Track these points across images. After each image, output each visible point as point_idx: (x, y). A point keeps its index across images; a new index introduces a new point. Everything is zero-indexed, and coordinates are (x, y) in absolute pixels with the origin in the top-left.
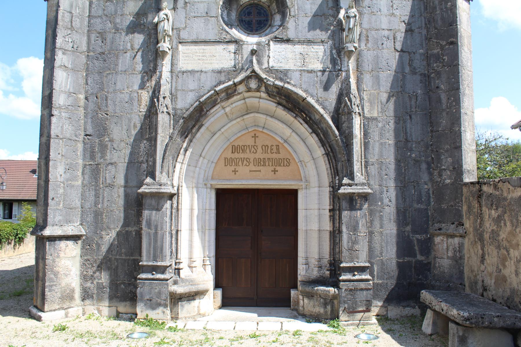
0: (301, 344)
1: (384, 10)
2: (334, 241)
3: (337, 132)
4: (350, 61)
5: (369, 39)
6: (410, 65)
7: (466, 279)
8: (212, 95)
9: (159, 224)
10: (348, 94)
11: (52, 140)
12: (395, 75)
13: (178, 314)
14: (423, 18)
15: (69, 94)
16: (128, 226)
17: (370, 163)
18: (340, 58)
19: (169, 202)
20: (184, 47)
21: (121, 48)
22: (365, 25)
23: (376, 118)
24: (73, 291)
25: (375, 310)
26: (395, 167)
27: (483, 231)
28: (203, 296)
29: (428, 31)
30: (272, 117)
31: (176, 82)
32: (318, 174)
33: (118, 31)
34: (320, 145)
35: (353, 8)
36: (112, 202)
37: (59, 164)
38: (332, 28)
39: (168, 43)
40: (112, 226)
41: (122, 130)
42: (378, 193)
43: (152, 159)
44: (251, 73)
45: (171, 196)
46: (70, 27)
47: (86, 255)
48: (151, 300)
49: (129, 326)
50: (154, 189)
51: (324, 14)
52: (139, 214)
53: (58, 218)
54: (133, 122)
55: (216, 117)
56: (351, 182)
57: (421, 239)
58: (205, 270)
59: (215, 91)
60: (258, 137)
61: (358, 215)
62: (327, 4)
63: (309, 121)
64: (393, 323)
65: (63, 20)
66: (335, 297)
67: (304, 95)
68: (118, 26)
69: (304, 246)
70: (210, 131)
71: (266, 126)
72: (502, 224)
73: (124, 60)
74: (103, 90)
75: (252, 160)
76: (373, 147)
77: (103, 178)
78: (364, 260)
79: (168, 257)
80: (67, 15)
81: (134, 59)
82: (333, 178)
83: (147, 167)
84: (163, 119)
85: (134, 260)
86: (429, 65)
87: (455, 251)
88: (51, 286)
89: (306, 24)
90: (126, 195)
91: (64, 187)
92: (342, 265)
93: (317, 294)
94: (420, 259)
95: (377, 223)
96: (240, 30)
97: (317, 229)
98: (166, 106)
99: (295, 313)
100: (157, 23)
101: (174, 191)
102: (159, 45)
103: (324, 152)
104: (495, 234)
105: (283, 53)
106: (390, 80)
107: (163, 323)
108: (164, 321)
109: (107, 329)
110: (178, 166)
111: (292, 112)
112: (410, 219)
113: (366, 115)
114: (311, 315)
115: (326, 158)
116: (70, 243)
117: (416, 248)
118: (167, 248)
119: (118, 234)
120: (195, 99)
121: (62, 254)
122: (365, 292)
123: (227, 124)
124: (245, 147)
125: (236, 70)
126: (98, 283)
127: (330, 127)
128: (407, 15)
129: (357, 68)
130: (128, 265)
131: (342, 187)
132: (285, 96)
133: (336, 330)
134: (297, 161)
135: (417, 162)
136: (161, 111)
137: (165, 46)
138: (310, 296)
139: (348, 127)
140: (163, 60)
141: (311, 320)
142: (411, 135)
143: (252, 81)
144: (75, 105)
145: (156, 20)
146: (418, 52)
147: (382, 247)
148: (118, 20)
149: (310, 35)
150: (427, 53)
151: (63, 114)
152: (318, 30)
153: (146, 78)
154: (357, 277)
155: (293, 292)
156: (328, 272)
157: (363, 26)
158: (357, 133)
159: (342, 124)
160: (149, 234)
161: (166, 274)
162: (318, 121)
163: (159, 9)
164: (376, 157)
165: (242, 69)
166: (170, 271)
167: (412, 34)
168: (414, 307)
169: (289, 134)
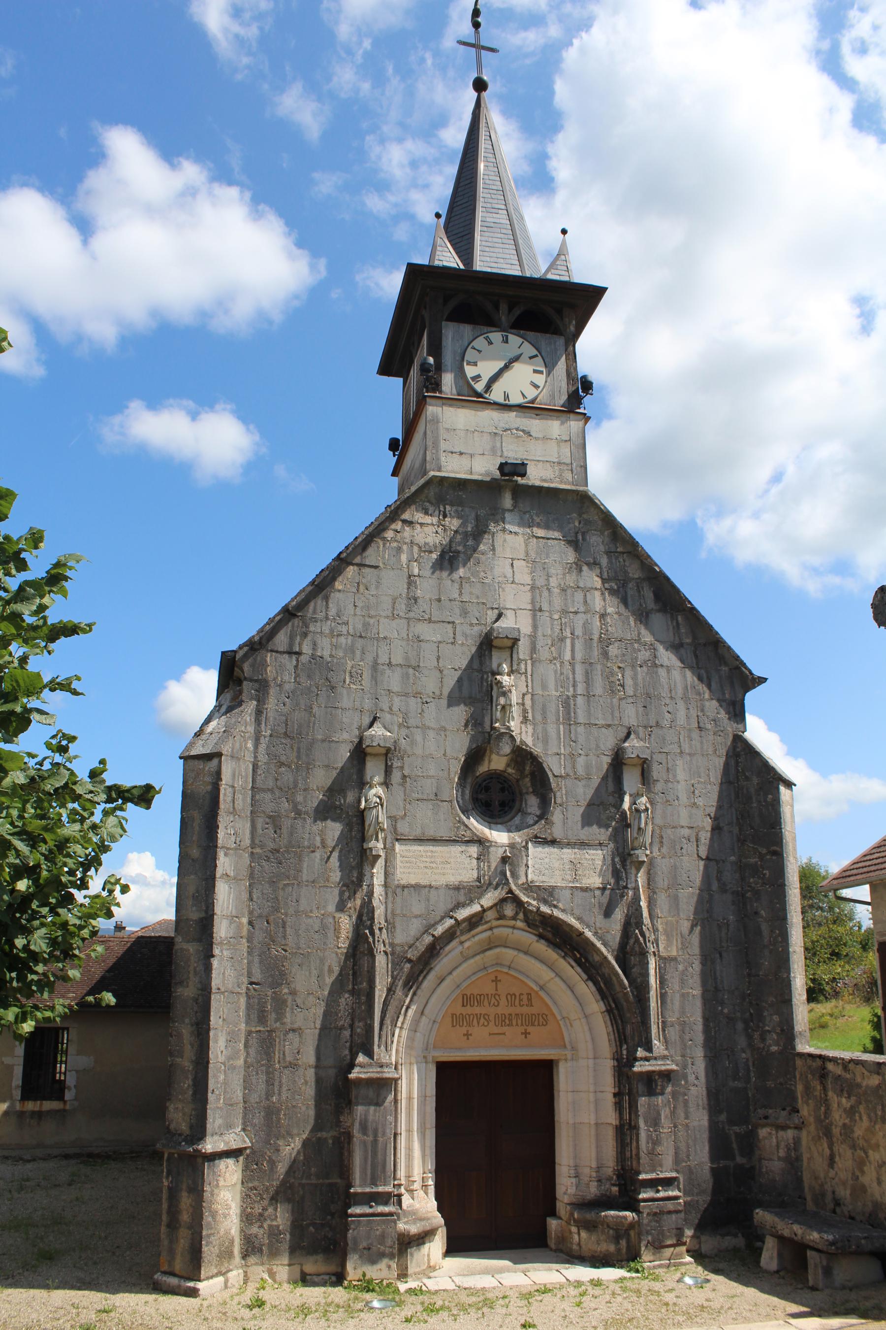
5: (664, 841)
7: (806, 1190)
9: (380, 1126)
10: (639, 924)
11: (213, 997)
12: (699, 895)
13: (407, 1268)
14: (733, 810)
15: (232, 918)
17: (669, 1024)
20: (403, 847)
21: (306, 843)
22: (659, 821)
24: (232, 1242)
27: (831, 1124)
29: (740, 830)
30: (526, 953)
31: (393, 903)
32: (593, 1039)
34: (599, 997)
36: (295, 1091)
37: (220, 1034)
38: (614, 823)
40: (295, 1131)
46: (232, 809)
47: (251, 1179)
48: (369, 1249)
51: (602, 803)
53: (219, 1121)
54: (327, 965)
56: (648, 1054)
61: (660, 1101)
65: (225, 800)
66: (632, 1225)
68: (300, 807)
71: (512, 965)
72: (857, 1118)
74: (277, 910)
75: (492, 1018)
76: (672, 1000)
77: (279, 1053)
80: (230, 790)
81: (326, 862)
83: (351, 1036)
84: (380, 962)
85: (331, 1185)
86: (743, 879)
87: (789, 1149)
88: (209, 1236)
90: (319, 1081)
91: (225, 1071)
95: (681, 1113)
96: (478, 818)
97: (593, 1122)
103: (604, 1009)
104: (847, 1130)
105: (547, 860)
111: (559, 948)
114: (593, 1257)
115: (608, 1018)
116: (230, 1161)
117: (735, 1146)
119: (305, 1144)
120: (422, 930)
121: (221, 1183)
122: (674, 1216)
123: (460, 965)
126: (270, 1226)
129: (649, 884)
134: (559, 1018)
135: (731, 1020)
137: (377, 846)
138: (590, 1226)
139: (640, 974)
140: (373, 867)
144: (238, 936)
147: (688, 1147)
148: (299, 798)
150: (740, 861)
151: (225, 953)
152: (595, 826)
153: (347, 894)
154: (661, 1194)
155: (553, 1224)
160: (364, 1143)
163: (362, 784)
164: (677, 1015)
165: (490, 884)
168: (736, 1236)
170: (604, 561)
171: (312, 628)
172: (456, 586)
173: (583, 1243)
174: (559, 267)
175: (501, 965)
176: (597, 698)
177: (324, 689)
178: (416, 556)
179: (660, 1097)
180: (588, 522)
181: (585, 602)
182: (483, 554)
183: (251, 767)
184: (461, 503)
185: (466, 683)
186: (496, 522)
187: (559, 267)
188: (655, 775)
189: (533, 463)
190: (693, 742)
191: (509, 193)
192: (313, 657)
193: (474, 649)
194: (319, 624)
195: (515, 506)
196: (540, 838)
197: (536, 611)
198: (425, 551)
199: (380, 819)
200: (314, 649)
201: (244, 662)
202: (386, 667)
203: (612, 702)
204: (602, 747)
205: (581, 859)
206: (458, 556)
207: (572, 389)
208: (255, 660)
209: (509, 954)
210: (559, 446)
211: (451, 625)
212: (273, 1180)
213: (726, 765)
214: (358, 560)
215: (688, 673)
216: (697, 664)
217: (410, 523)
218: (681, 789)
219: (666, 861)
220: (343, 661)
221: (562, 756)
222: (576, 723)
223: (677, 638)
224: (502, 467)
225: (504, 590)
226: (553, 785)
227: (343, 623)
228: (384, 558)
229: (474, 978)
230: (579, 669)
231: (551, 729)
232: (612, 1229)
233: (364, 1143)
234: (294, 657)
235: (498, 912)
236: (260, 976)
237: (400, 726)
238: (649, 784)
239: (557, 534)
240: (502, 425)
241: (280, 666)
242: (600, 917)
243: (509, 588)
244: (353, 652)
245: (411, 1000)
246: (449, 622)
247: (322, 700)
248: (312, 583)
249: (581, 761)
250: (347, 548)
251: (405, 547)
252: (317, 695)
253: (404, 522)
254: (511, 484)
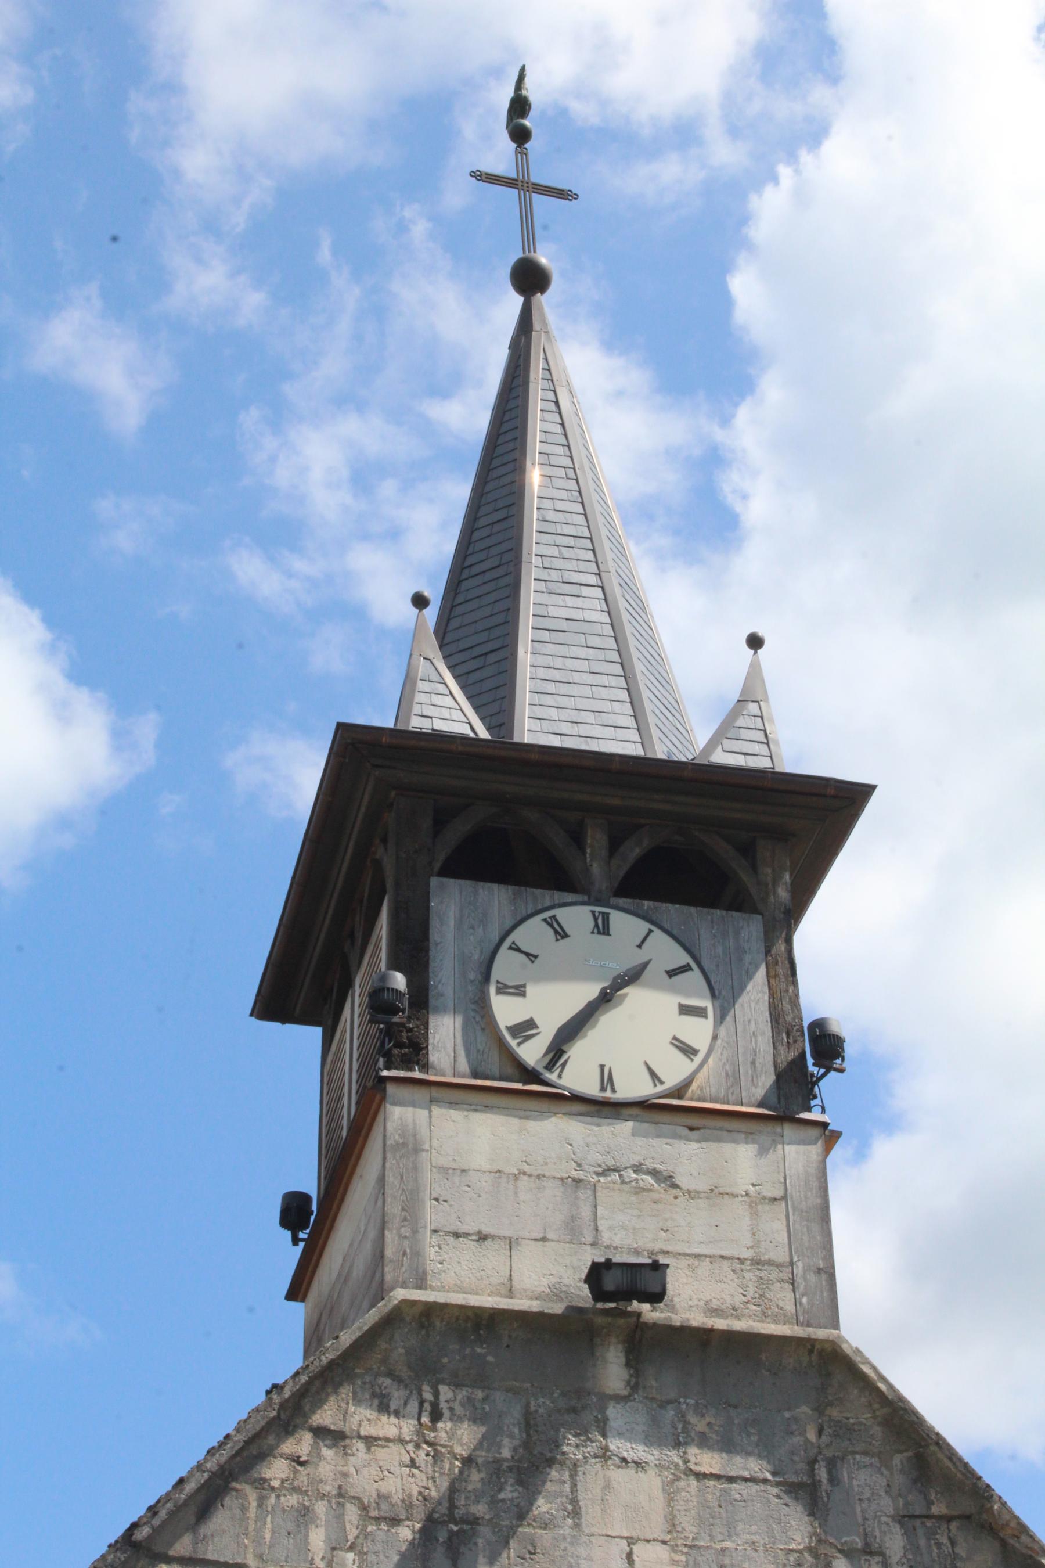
170: (895, 1543)
174: (744, 734)
178: (352, 1533)
180: (843, 1430)
182: (545, 1526)
184: (481, 1379)
186: (582, 1432)
187: (744, 734)
189: (684, 1262)
191: (607, 544)
195: (634, 1387)
198: (378, 1520)
206: (475, 1534)
207: (787, 1056)
210: (755, 1214)
217: (336, 1437)
224: (596, 1274)
228: (258, 1540)
239: (755, 1466)
240: (595, 1157)
250: (153, 1510)
251: (321, 1508)
253: (321, 1432)
254: (621, 1321)
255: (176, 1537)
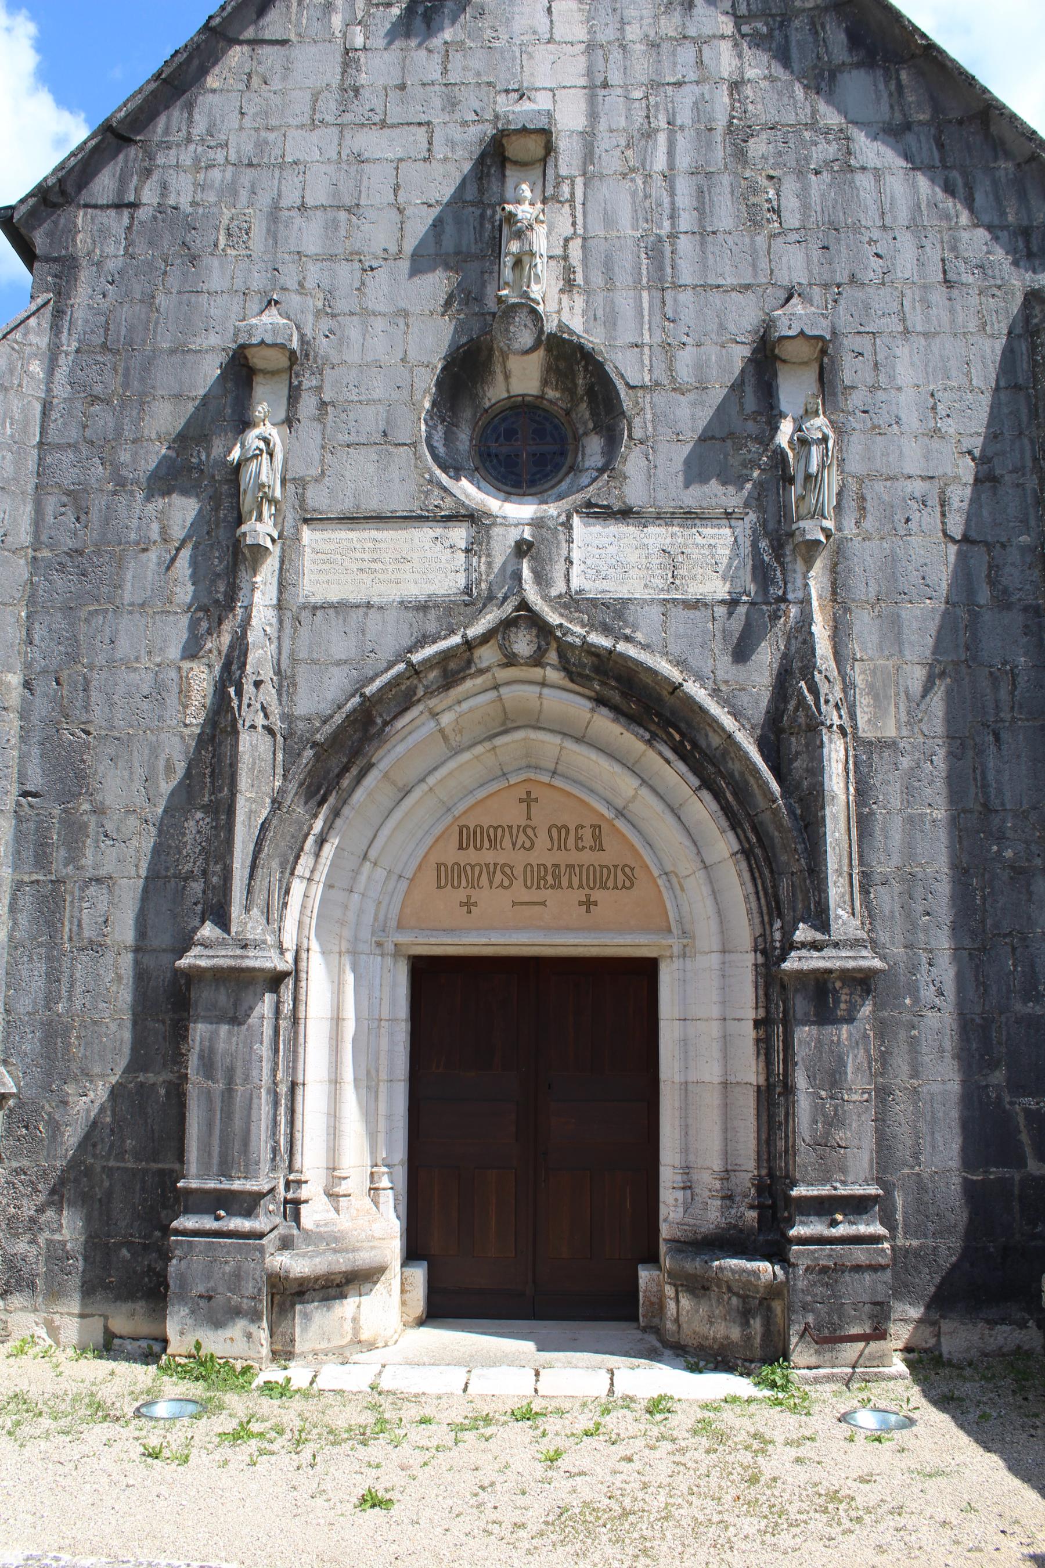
0: (673, 1440)
1: (911, 420)
2: (771, 1117)
3: (775, 786)
4: (812, 573)
5: (868, 505)
6: (992, 583)
8: (399, 676)
10: (808, 669)
12: (945, 614)
13: (293, 1341)
14: (1026, 441)
16: (145, 1069)
17: (878, 879)
18: (782, 564)
19: (269, 998)
20: (318, 535)
21: (133, 536)
22: (855, 465)
23: (894, 743)
25: (900, 1334)
26: (953, 889)
28: (369, 1286)
30: (579, 740)
31: (293, 639)
32: (719, 912)
33: (123, 486)
34: (725, 824)
35: (817, 414)
36: (99, 994)
38: (756, 474)
39: (271, 523)
40: (97, 1070)
41: (132, 780)
42: (902, 969)
43: (218, 868)
44: (517, 609)
45: (275, 980)
49: (141, 1377)
50: (223, 958)
51: (731, 435)
52: (179, 1034)
54: (163, 757)
55: (410, 741)
56: (819, 936)
57: (1039, 1110)
58: (376, 1204)
59: (410, 664)
60: (536, 800)
61: (844, 1035)
62: (741, 404)
63: (691, 752)
64: (959, 1376)
66: (775, 1291)
67: (674, 674)
68: (124, 472)
69: (677, 1131)
70: (394, 783)
73: (141, 575)
75: (518, 871)
76: (884, 829)
77: (71, 923)
78: (862, 1176)
79: (265, 1167)
81: (168, 568)
82: (766, 925)
83: (204, 892)
85: (161, 1173)
89: (678, 464)
90: (141, 976)
92: (794, 1193)
93: (719, 1282)
94: (1038, 1173)
95: (900, 1063)
96: (483, 484)
97: (717, 1080)
98: (263, 708)
99: (652, 1340)
100: (239, 465)
101: (285, 964)
102: (244, 528)
103: (736, 847)
105: (612, 550)
106: (933, 627)
107: (246, 1370)
108: (249, 1362)
109: (73, 1388)
110: (298, 888)
112: (1004, 1050)
113: (861, 734)
114: (701, 1347)
115: (744, 865)
117: (1024, 1137)
118: (263, 1137)
119: (115, 1093)
120: (350, 689)
122: (867, 1277)
123: (443, 763)
124: (500, 830)
125: (472, 601)
126: (49, 1242)
127: (755, 771)
128: (978, 434)
129: (834, 593)
130: (143, 1189)
131: (793, 954)
132: (618, 679)
133: (781, 1395)
136: (247, 724)
137: (261, 529)
138: (698, 1286)
139: (807, 770)
141: (702, 1364)
142: (1000, 791)
143: (520, 635)
145: (235, 454)
146: (1014, 542)
147: (917, 1135)
148: (124, 457)
149: (692, 497)
152: (713, 481)
153: (205, 625)
154: (842, 1230)
155: (645, 1275)
156: (753, 1214)
157: (847, 468)
158: (835, 788)
159: (791, 761)
160: (209, 1095)
161: (257, 1216)
162: (718, 753)
163: (244, 424)
164: (896, 860)
165: (491, 598)
166: (271, 1207)
167: (994, 489)
168: (1022, 1325)
169: (631, 793)
171: (160, 160)
172: (437, 58)
173: (683, 1319)
175: (537, 768)
176: (720, 236)
177: (178, 261)
179: (845, 1026)
181: (700, 63)
183: (38, 407)
185: (450, 229)
188: (848, 376)
190: (934, 311)
192: (161, 208)
193: (467, 167)
194: (173, 152)
196: (597, 506)
197: (596, 87)
199: (263, 478)
200: (163, 195)
201: (34, 228)
202: (295, 213)
203: (753, 242)
204: (733, 329)
205: (686, 545)
208: (56, 223)
209: (549, 742)
211: (424, 129)
212: (55, 1158)
213: (1009, 354)
214: (249, 33)
215: (923, 182)
216: (942, 160)
218: (907, 404)
219: (873, 545)
220: (214, 210)
221: (646, 350)
222: (676, 286)
223: (898, 116)
225: (531, 56)
226: (627, 404)
227: (220, 146)
228: (298, 24)
229: (481, 794)
230: (684, 187)
231: (624, 301)
232: (737, 1295)
233: (209, 1095)
234: (126, 213)
235: (500, 647)
236: (40, 781)
237: (318, 314)
238: (834, 394)
241: (100, 231)
242: (725, 661)
243: (542, 52)
244: (235, 194)
245: (329, 826)
246: (420, 124)
247: (173, 281)
248: (157, 76)
249: (685, 358)
252: (166, 272)
255: (245, 28)
